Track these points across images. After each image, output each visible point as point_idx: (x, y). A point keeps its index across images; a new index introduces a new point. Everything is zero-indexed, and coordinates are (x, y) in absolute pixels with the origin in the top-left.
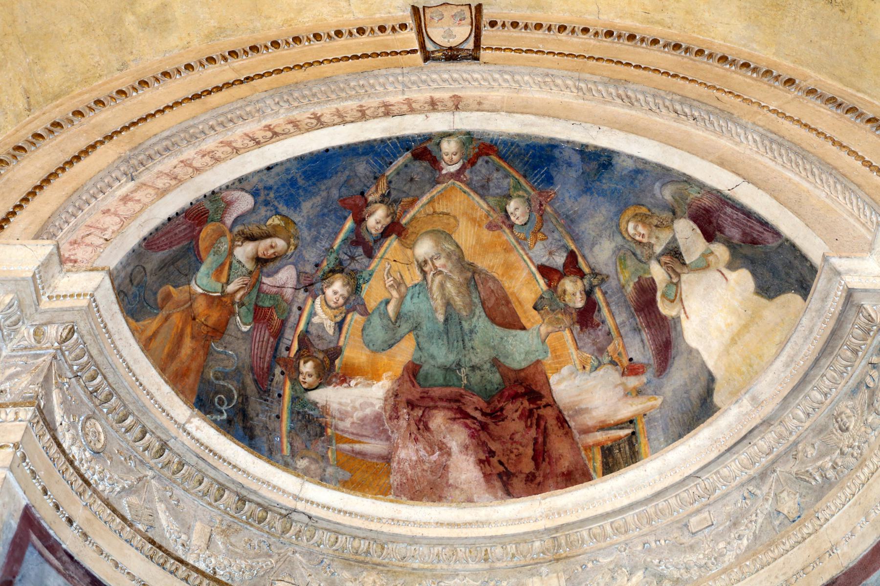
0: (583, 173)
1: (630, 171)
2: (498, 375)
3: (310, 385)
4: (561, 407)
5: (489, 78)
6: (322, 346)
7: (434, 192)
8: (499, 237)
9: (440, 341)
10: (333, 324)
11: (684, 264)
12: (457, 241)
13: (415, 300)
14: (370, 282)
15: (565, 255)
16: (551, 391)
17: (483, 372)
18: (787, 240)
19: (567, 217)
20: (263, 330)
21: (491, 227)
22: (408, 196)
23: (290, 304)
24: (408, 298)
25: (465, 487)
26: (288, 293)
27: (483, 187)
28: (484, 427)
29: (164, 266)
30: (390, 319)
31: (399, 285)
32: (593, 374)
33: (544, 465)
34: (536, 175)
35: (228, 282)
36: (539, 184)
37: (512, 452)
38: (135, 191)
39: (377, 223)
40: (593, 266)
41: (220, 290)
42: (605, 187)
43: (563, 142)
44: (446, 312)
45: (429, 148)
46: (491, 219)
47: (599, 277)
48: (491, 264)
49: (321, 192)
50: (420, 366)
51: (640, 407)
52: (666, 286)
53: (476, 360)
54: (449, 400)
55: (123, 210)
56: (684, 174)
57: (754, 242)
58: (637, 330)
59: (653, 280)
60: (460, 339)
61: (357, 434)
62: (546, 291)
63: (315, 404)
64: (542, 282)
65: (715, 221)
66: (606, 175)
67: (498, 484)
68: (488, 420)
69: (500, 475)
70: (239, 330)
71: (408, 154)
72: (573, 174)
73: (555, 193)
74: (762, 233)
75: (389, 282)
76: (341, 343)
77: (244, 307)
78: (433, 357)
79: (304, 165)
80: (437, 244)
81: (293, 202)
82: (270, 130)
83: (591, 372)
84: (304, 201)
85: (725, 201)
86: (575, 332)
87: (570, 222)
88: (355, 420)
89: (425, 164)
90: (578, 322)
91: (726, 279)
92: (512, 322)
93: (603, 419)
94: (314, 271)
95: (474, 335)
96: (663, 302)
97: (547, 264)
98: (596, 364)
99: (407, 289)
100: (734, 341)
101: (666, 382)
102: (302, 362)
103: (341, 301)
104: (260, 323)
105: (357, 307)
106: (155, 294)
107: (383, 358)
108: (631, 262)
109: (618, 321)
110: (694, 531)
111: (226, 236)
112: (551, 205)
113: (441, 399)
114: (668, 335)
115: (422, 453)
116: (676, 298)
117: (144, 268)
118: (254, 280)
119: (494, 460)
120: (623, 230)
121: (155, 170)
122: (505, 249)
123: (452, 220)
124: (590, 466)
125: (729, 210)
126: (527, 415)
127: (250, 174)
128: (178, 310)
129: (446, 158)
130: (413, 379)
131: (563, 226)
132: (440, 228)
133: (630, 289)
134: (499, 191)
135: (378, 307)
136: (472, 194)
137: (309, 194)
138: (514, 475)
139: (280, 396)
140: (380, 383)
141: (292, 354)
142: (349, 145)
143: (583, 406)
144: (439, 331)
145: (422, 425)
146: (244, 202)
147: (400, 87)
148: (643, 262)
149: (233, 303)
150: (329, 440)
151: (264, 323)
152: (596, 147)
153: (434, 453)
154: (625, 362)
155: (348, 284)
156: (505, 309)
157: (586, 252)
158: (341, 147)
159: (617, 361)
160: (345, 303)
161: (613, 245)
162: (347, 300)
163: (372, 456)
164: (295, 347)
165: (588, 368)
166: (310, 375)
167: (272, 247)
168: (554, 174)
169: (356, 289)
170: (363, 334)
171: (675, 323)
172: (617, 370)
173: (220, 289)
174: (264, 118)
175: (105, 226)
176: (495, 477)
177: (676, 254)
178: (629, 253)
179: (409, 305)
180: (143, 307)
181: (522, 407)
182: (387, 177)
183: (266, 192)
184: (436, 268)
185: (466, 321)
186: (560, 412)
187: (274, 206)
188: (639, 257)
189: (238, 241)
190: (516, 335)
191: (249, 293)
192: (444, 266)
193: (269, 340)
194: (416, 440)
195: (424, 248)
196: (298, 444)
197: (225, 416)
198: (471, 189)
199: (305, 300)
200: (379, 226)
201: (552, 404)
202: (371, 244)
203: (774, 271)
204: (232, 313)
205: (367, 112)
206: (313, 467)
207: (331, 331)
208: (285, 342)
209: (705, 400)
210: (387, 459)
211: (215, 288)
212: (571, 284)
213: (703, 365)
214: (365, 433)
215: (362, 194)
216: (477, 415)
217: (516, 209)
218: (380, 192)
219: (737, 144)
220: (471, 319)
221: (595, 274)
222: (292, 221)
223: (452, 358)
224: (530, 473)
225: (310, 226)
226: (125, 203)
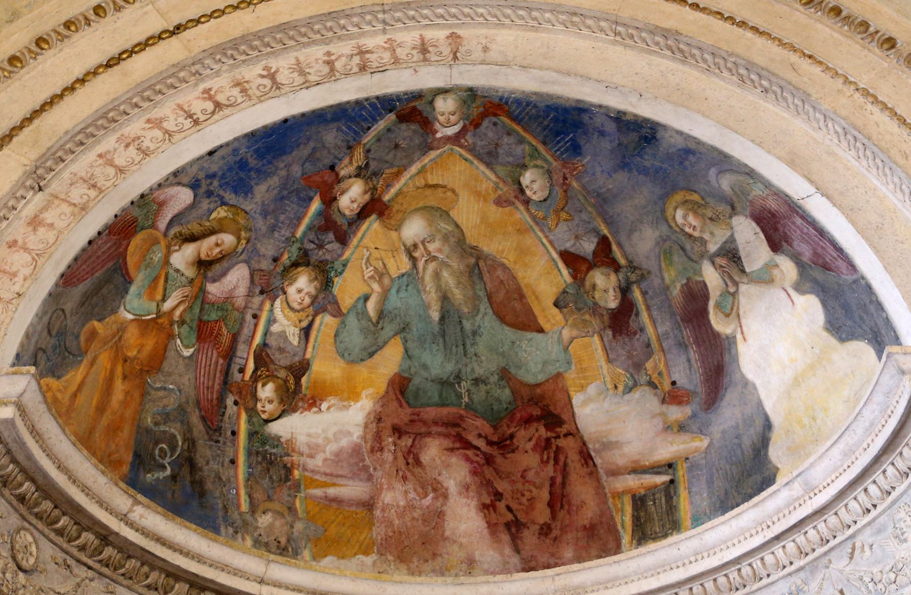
0: (619, 145)
1: (679, 150)
2: (507, 391)
3: (271, 414)
4: (586, 438)
5: (498, 13)
7: (426, 160)
8: (511, 215)
9: (434, 346)
10: (297, 331)
11: (743, 271)
12: (456, 219)
13: (403, 294)
14: (344, 274)
15: (595, 240)
17: (489, 387)
18: (863, 278)
19: (599, 195)
20: (210, 353)
21: (499, 202)
22: (392, 166)
23: (243, 311)
24: (393, 291)
25: (464, 540)
27: (489, 153)
28: (489, 460)
29: (87, 298)
30: (371, 320)
31: (381, 275)
32: (627, 397)
33: (561, 514)
34: (558, 142)
35: (164, 300)
36: (562, 154)
37: (523, 495)
38: (45, 209)
39: (352, 202)
40: (630, 258)
41: (155, 310)
42: (647, 164)
43: (595, 106)
44: (442, 307)
45: (419, 108)
46: (500, 192)
47: (637, 271)
48: (500, 248)
49: (279, 172)
50: (409, 380)
51: (682, 447)
52: (721, 295)
53: (480, 371)
54: (446, 424)
55: (33, 241)
56: (746, 165)
57: (826, 267)
58: (682, 345)
60: (460, 343)
61: (331, 475)
62: (571, 285)
63: (278, 438)
64: (565, 272)
65: (781, 229)
66: (647, 150)
67: (505, 537)
68: (494, 451)
69: (508, 525)
70: (181, 356)
71: (392, 117)
72: (606, 145)
73: (583, 165)
74: (836, 259)
75: (369, 272)
76: (308, 356)
77: (185, 326)
78: (425, 367)
79: (256, 141)
80: (430, 223)
81: (243, 188)
82: (210, 98)
83: (624, 394)
84: (257, 184)
85: (794, 208)
86: (605, 339)
88: (328, 455)
89: (414, 127)
90: (610, 327)
91: (792, 301)
93: (636, 458)
94: (272, 267)
95: (478, 338)
96: (716, 314)
97: (572, 250)
98: (631, 383)
99: (392, 280)
100: (797, 382)
101: (714, 420)
102: (260, 385)
103: (307, 301)
104: (205, 342)
105: (329, 308)
106: (77, 337)
107: (362, 371)
108: (678, 258)
109: (660, 330)
111: (159, 243)
112: (578, 178)
114: (720, 358)
115: (412, 495)
116: (731, 311)
117: (63, 311)
118: (196, 289)
119: (501, 505)
120: (670, 218)
121: (66, 175)
122: (519, 230)
123: (449, 194)
124: (618, 520)
125: (799, 221)
127: (187, 164)
128: (106, 347)
129: (442, 119)
130: (400, 396)
131: (593, 206)
132: (434, 203)
133: (676, 291)
134: (511, 159)
135: (354, 306)
136: (476, 162)
137: (262, 174)
138: (524, 525)
139: (234, 433)
140: (359, 404)
141: (247, 376)
142: (314, 112)
143: (614, 439)
144: (433, 333)
145: (412, 458)
146: (183, 197)
147: (380, 26)
148: (694, 261)
149: (172, 323)
150: (297, 487)
151: (211, 342)
152: (636, 116)
153: (426, 495)
154: (667, 386)
155: (316, 278)
156: (517, 305)
157: (623, 238)
159: (656, 382)
160: (312, 303)
161: (657, 234)
162: (314, 299)
163: (351, 502)
164: (251, 366)
165: (621, 388)
166: (270, 402)
168: (582, 142)
169: (326, 284)
170: (335, 341)
171: (729, 344)
172: (656, 395)
174: (202, 80)
175: (14, 269)
176: (502, 528)
177: (734, 257)
178: (677, 247)
179: (394, 301)
180: (64, 358)
181: (537, 435)
182: (365, 145)
183: (209, 181)
184: (429, 253)
185: (467, 319)
186: (584, 444)
187: (218, 195)
188: (690, 254)
189: (175, 245)
190: (532, 339)
191: (191, 308)
192: (440, 250)
193: (217, 362)
194: (405, 478)
196: (259, 496)
197: (168, 472)
198: (475, 156)
199: (262, 304)
200: (355, 205)
201: (574, 433)
202: (345, 227)
203: (846, 308)
204: (171, 336)
205: (338, 65)
206: (278, 523)
207: (295, 341)
208: (238, 362)
209: (759, 451)
210: (369, 505)
212: (603, 277)
213: (760, 404)
214: (340, 473)
215: (332, 168)
216: (481, 443)
217: (533, 181)
218: (355, 164)
219: (814, 129)
220: (474, 317)
221: (632, 266)
222: (242, 210)
223: (450, 367)
224: (545, 524)
225: (265, 214)
226: (35, 230)
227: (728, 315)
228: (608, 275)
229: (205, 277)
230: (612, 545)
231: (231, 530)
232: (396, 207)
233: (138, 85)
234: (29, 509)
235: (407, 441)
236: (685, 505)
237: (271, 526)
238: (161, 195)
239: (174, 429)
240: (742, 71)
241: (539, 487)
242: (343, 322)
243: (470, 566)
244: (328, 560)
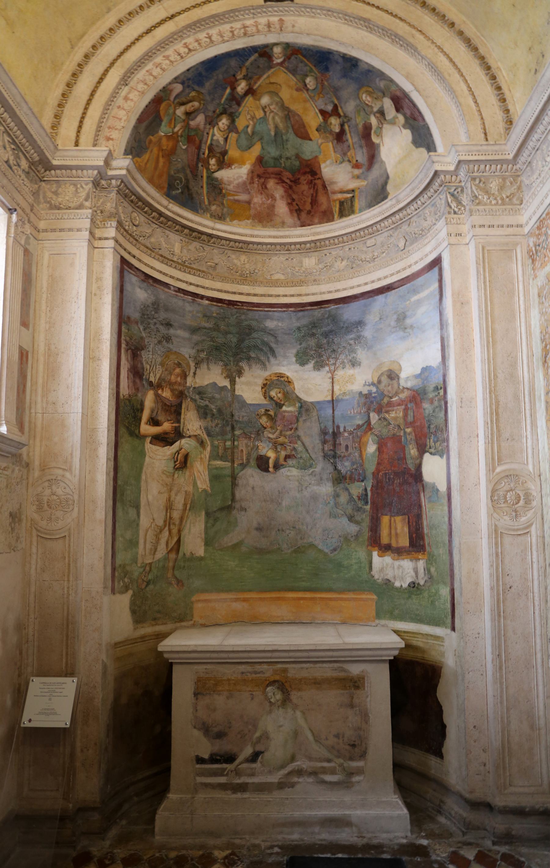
2: (298, 162)
6: (219, 151)
11: (385, 119)
15: (332, 105)
16: (321, 172)
21: (298, 90)
23: (203, 132)
24: (258, 124)
25: (281, 215)
26: (202, 126)
27: (294, 70)
28: (291, 187)
29: (147, 128)
30: (249, 135)
32: (340, 165)
33: (315, 207)
35: (175, 127)
38: (129, 93)
42: (353, 75)
50: (263, 158)
53: (289, 155)
54: (276, 174)
57: (415, 119)
58: (361, 147)
59: (371, 124)
63: (217, 179)
64: (321, 117)
67: (295, 214)
69: (296, 210)
72: (338, 67)
75: (249, 117)
76: (227, 148)
78: (269, 153)
81: (200, 83)
83: (339, 164)
85: (406, 96)
86: (334, 144)
87: (336, 90)
88: (235, 185)
89: (265, 59)
92: (305, 136)
97: (324, 109)
99: (257, 119)
100: (400, 162)
102: (210, 159)
103: (226, 127)
106: (145, 142)
107: (246, 154)
108: (362, 113)
110: (368, 246)
112: (327, 81)
113: (272, 173)
115: (264, 199)
116: (379, 134)
119: (294, 203)
120: (360, 97)
123: (279, 86)
125: (407, 100)
126: (310, 182)
129: (276, 55)
132: (273, 90)
133: (360, 126)
135: (243, 130)
136: (289, 73)
139: (202, 177)
140: (245, 167)
143: (334, 180)
145: (264, 186)
146: (178, 88)
148: (368, 114)
149: (178, 136)
150: (224, 196)
153: (269, 199)
154: (354, 162)
157: (343, 105)
158: (223, 54)
162: (229, 127)
164: (207, 152)
165: (338, 162)
166: (214, 165)
167: (193, 106)
169: (233, 121)
173: (171, 130)
175: (120, 117)
176: (294, 211)
179: (258, 128)
186: (324, 182)
191: (184, 131)
192: (275, 109)
194: (261, 193)
195: (265, 100)
197: (180, 191)
199: (210, 129)
200: (243, 91)
201: (321, 178)
202: (239, 99)
204: (178, 141)
206: (218, 209)
207: (222, 143)
210: (249, 203)
211: (169, 132)
213: (386, 170)
214: (239, 191)
215: (234, 76)
216: (288, 181)
217: (310, 82)
218: (243, 74)
221: (345, 116)
223: (278, 153)
225: (210, 94)
226: (126, 101)
227: (378, 136)
228: (336, 119)
229: (189, 119)
230: (331, 218)
231: (202, 211)
232: (258, 91)
233: (159, 42)
234: (135, 205)
235: (262, 180)
236: (357, 205)
237: (216, 210)
238: (171, 87)
239: (181, 175)
240: (393, 37)
241: (308, 197)
242: (239, 136)
243: (283, 224)
244: (235, 222)
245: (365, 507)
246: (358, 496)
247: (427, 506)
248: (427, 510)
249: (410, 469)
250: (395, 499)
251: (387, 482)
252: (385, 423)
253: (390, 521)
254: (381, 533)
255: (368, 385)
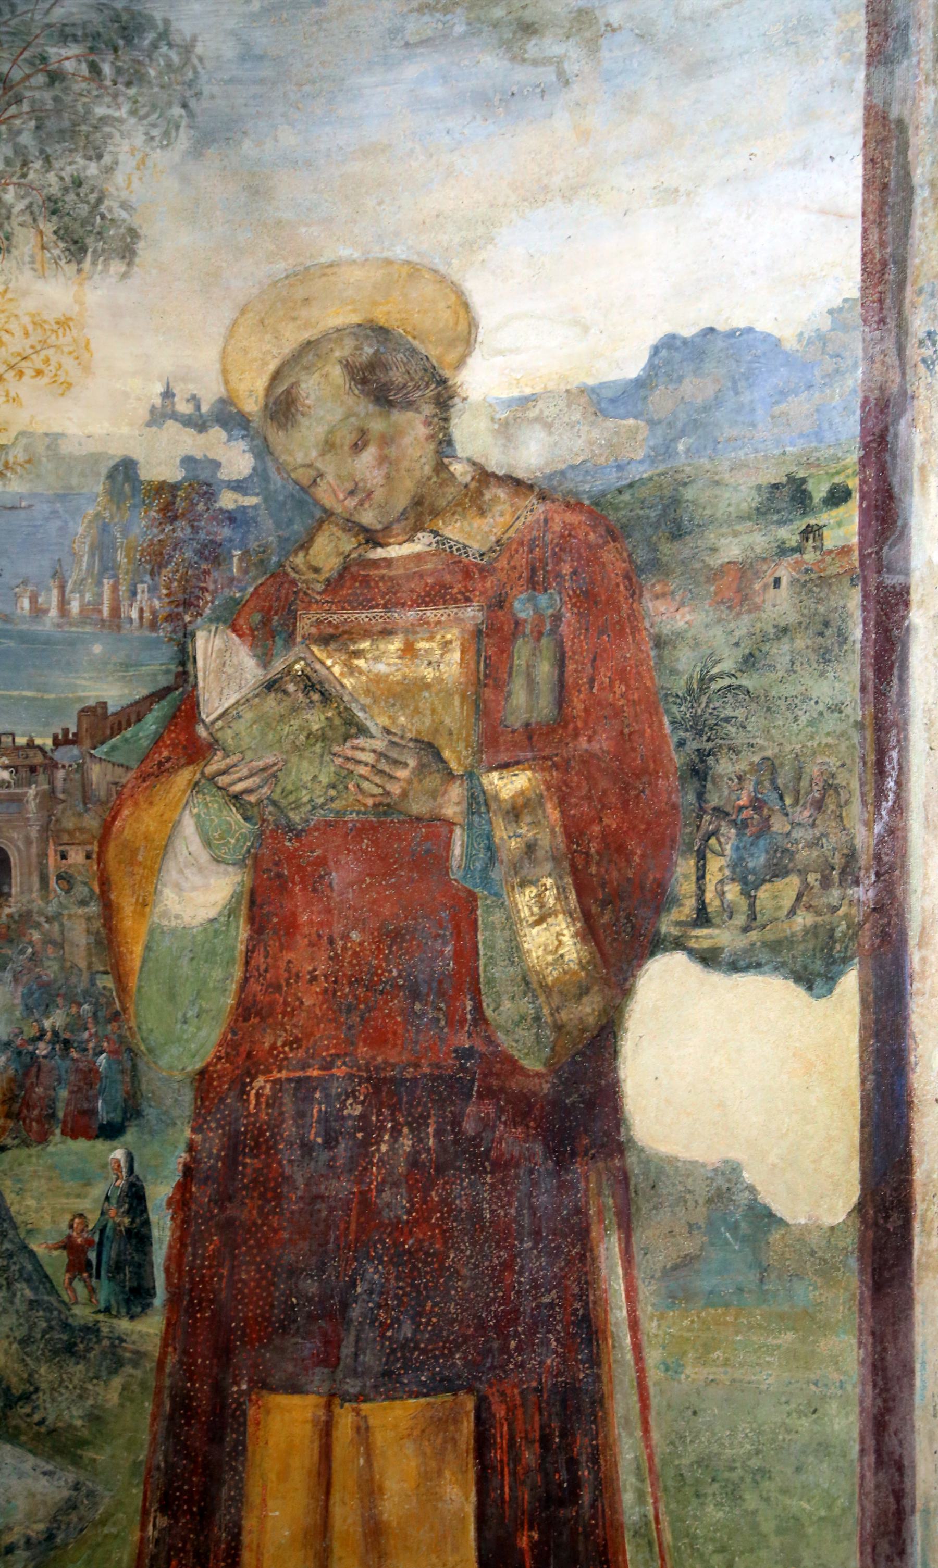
245: (124, 1325)
246: (68, 1245)
247: (649, 1326)
248: (653, 1356)
249: (511, 1061)
250: (373, 1273)
251: (307, 1148)
252: (316, 720)
253: (326, 1431)
254: (250, 1523)
255: (187, 422)
